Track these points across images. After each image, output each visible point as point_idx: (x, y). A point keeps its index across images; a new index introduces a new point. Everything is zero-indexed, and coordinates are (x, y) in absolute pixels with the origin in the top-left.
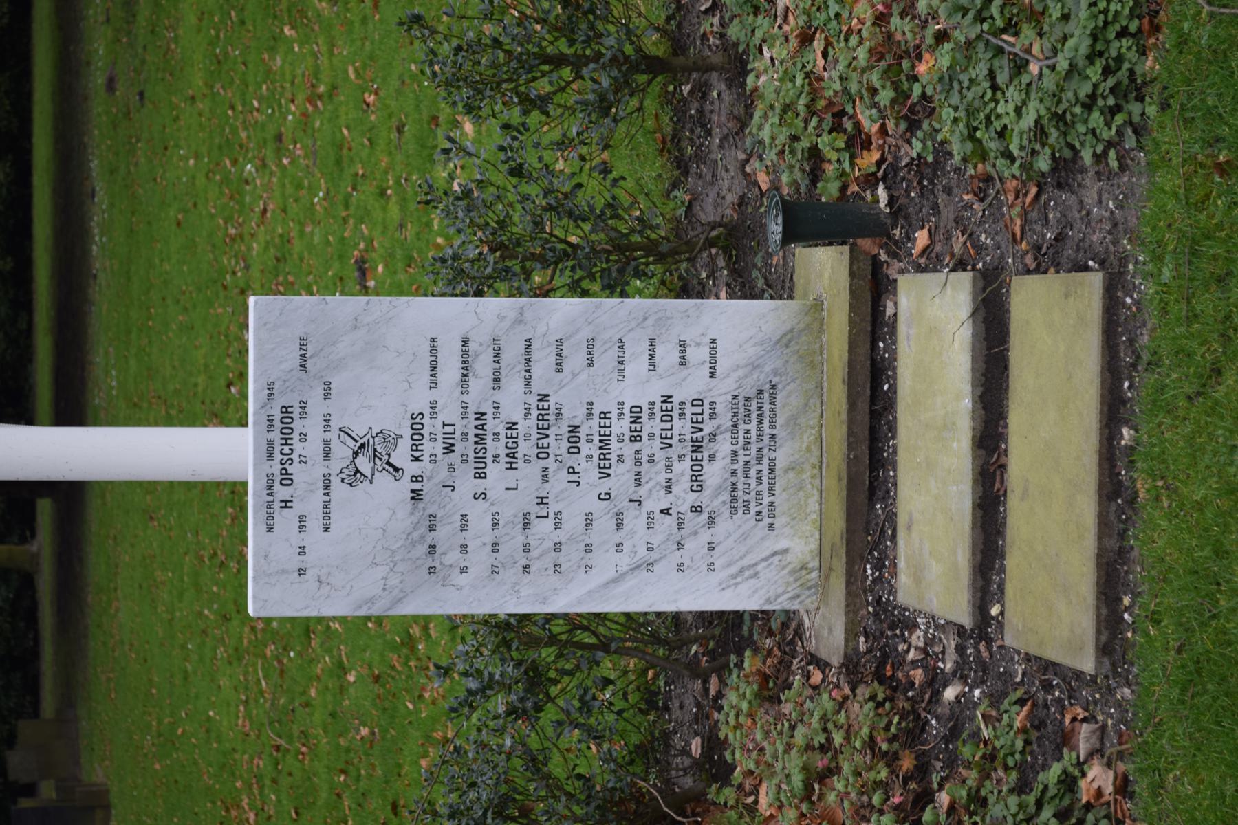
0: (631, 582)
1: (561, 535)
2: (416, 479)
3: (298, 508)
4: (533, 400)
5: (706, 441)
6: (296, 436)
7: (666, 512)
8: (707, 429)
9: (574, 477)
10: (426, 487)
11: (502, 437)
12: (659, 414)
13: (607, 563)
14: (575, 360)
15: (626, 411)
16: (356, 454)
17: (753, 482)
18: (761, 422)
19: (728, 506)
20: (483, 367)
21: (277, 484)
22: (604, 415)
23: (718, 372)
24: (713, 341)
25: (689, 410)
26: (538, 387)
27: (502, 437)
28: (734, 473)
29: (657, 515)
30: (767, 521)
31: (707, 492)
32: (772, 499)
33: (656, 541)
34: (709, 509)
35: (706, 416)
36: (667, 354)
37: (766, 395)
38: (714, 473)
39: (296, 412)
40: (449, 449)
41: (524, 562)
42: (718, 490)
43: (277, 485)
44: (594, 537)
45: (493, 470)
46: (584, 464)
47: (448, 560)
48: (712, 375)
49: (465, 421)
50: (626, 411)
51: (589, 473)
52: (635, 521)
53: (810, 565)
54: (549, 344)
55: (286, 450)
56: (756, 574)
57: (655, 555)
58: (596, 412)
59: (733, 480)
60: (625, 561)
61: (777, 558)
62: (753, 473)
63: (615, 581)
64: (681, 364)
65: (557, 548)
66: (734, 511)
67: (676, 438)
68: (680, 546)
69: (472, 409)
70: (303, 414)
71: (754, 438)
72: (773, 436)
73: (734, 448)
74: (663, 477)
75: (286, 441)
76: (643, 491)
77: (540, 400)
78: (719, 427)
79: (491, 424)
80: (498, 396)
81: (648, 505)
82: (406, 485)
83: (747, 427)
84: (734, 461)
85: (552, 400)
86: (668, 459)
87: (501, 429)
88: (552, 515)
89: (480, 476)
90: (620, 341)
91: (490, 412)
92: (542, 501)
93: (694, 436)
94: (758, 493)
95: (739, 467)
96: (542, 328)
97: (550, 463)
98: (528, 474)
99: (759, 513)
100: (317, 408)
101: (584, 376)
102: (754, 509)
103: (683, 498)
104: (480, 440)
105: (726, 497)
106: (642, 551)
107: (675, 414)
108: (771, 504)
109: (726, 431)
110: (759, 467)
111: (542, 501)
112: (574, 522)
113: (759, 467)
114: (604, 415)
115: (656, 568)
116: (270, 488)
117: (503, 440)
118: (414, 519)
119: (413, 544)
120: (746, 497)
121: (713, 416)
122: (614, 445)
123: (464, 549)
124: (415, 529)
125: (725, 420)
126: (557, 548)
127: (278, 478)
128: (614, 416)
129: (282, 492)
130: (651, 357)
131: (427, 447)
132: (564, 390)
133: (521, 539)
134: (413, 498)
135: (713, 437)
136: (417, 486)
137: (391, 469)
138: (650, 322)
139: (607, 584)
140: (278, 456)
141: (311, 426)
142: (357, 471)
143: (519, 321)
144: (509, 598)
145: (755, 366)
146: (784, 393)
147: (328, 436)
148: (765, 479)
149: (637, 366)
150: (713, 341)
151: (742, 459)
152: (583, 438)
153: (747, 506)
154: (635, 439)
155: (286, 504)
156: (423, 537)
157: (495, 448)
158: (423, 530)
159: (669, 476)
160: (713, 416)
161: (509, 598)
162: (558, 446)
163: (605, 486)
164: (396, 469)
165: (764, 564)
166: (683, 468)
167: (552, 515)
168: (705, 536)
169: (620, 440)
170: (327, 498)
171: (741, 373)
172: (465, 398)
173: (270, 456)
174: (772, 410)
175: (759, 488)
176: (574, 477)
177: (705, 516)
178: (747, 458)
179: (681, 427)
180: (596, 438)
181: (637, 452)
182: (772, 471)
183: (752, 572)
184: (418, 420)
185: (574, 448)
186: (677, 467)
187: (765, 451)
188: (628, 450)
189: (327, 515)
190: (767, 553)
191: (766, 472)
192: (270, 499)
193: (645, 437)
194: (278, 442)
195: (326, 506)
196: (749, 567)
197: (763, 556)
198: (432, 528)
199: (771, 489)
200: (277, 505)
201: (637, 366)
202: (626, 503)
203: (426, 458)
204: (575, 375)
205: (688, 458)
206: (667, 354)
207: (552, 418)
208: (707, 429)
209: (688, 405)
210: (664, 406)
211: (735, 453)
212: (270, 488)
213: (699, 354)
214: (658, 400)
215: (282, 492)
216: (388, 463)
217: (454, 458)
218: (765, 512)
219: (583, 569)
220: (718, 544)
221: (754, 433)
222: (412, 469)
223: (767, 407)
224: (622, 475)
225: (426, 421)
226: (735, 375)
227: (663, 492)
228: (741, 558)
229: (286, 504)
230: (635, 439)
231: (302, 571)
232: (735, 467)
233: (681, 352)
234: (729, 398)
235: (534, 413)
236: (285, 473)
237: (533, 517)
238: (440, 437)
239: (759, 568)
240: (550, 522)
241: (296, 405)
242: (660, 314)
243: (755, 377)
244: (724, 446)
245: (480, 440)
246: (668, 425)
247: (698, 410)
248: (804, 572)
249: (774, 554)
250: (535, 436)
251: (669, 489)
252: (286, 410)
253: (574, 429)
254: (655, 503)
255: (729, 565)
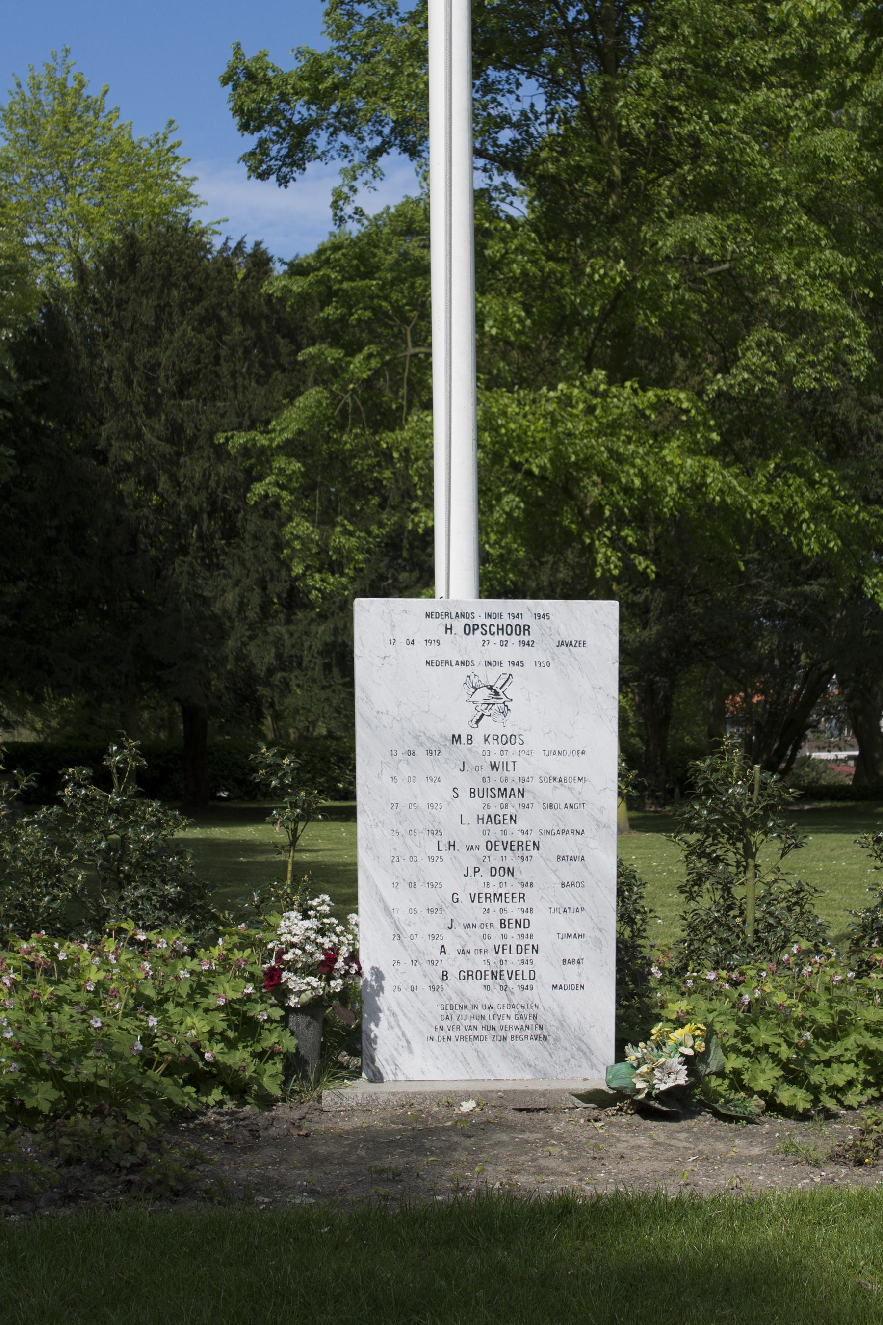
0: (384, 920)
1: (423, 862)
2: (470, 738)
3: (446, 638)
4: (534, 837)
5: (501, 982)
6: (505, 637)
7: (443, 950)
8: (511, 983)
9: (471, 872)
10: (463, 747)
11: (504, 811)
12: (523, 942)
13: (400, 900)
14: (568, 872)
15: (526, 916)
16: (491, 688)
17: (467, 1023)
18: (517, 1028)
19: (448, 1002)
20: (562, 795)
21: (465, 621)
22: (522, 897)
23: (557, 991)
24: (582, 987)
25: (526, 968)
26: (546, 841)
27: (504, 811)
28: (475, 1007)
29: (440, 943)
30: (435, 1035)
31: (459, 984)
32: (453, 1039)
33: (419, 942)
34: (445, 986)
35: (521, 982)
36: (572, 949)
37: (538, 1032)
38: (474, 990)
39: (526, 638)
40: (494, 767)
41: (401, 831)
42: (461, 994)
43: (464, 621)
44: (421, 889)
45: (477, 804)
46: (482, 880)
47: (403, 766)
48: (555, 987)
49: (517, 780)
50: (526, 916)
51: (475, 885)
52: (436, 924)
53: (398, 1072)
54: (580, 850)
55: (494, 629)
56: (392, 1027)
57: (406, 941)
58: (526, 890)
59: (469, 1006)
60: (402, 916)
61: (405, 1044)
62: (475, 1022)
63: (386, 908)
64: (564, 961)
65: (414, 859)
66: (444, 1007)
67: (503, 957)
68: (415, 962)
69: (527, 786)
70: (524, 643)
71: (503, 1023)
72: (505, 1039)
73: (495, 1006)
74: (471, 947)
75: (501, 629)
76: (459, 930)
77: (534, 843)
78: (512, 993)
79: (515, 801)
80: (538, 808)
81: (447, 934)
82: (464, 731)
83: (512, 1017)
84: (484, 1007)
85: (534, 853)
86: (486, 951)
87: (510, 811)
88: (439, 854)
89: (472, 792)
90: (583, 909)
91: (525, 801)
92: (452, 845)
93: (505, 973)
94: (458, 1028)
95: (481, 1011)
96: (593, 844)
97: (483, 851)
98: (474, 834)
99: (442, 1028)
100: (528, 655)
101: (554, 879)
102: (446, 1024)
103: (454, 964)
104: (502, 792)
105: (456, 1001)
106: (409, 931)
107: (523, 956)
108: (449, 1039)
109: (509, 1000)
110: (479, 1028)
111: (452, 845)
112: (434, 872)
113: (479, 1028)
114: (522, 897)
115: (396, 941)
116: (463, 615)
117: (501, 813)
118: (437, 738)
119: (417, 737)
120: (454, 1017)
121: (523, 988)
122: (498, 905)
123: (411, 779)
124: (429, 738)
125: (519, 997)
126: (414, 859)
127: (470, 622)
128: (522, 905)
129: (458, 625)
130: (569, 936)
131: (496, 748)
132: (543, 864)
133: (420, 827)
134: (454, 736)
135: (505, 988)
136: (464, 739)
137: (478, 717)
138: (598, 934)
139: (382, 900)
140: (488, 622)
141: (514, 651)
142: (476, 689)
143: (599, 824)
144: (372, 818)
145: (562, 1024)
146: (540, 1047)
147: (505, 664)
148: (469, 1033)
149: (564, 924)
150: (582, 987)
151: (486, 1013)
152: (503, 880)
153: (447, 1018)
154: (503, 923)
155: (449, 629)
156: (422, 744)
157: (495, 806)
158: (428, 746)
159: (472, 952)
160: (523, 988)
161: (372, 818)
162: (497, 859)
163: (464, 898)
164: (478, 722)
165: (400, 1034)
166: (478, 963)
167: (439, 854)
168: (424, 984)
169: (502, 910)
170: (454, 663)
171: (557, 1010)
172: (537, 780)
173: (489, 616)
174: (526, 1037)
175: (462, 1028)
176: (471, 872)
177: (439, 983)
178: (487, 1018)
179: (512, 962)
180: (503, 891)
181: (492, 925)
182: (476, 1038)
183: (393, 1023)
184: (518, 740)
185: (494, 872)
186: (480, 958)
187: (493, 1032)
188: (495, 918)
189: (439, 664)
190: (409, 1035)
191: (475, 1033)
192: (454, 616)
193: (504, 931)
194: (500, 622)
195: (448, 663)
196: (397, 1021)
197: (406, 1032)
198: (430, 752)
199: (462, 1038)
200: (448, 621)
201: (564, 924)
202: (450, 917)
203: (487, 747)
204: (555, 871)
205: (486, 967)
206: (572, 949)
207: (520, 853)
208: (511, 983)
209: (530, 967)
210: (530, 947)
211: (491, 1007)
212: (463, 615)
213: (572, 974)
214: (533, 942)
215: (458, 625)
216: (483, 715)
217: (487, 771)
218: (442, 1033)
219: (396, 881)
220: (416, 994)
221: (506, 1022)
222: (478, 735)
223: (529, 1033)
224: (473, 912)
225: (517, 747)
226: (555, 1006)
227: (460, 948)
228: (405, 1014)
229: (449, 629)
230: (503, 923)
231: (393, 642)
232: (480, 1007)
233: (574, 960)
234: (537, 1002)
235: (524, 838)
236: (475, 628)
237: (438, 838)
238: (504, 759)
239: (397, 1030)
240: (434, 852)
241: (530, 638)
242: (604, 942)
243: (553, 1023)
244: (497, 998)
245: (502, 792)
246: (514, 950)
247: (526, 976)
248: (393, 1067)
249: (408, 1042)
250: (505, 839)
251: (465, 952)
252: (526, 629)
253: (510, 872)
254: (451, 942)
255: (399, 1005)
